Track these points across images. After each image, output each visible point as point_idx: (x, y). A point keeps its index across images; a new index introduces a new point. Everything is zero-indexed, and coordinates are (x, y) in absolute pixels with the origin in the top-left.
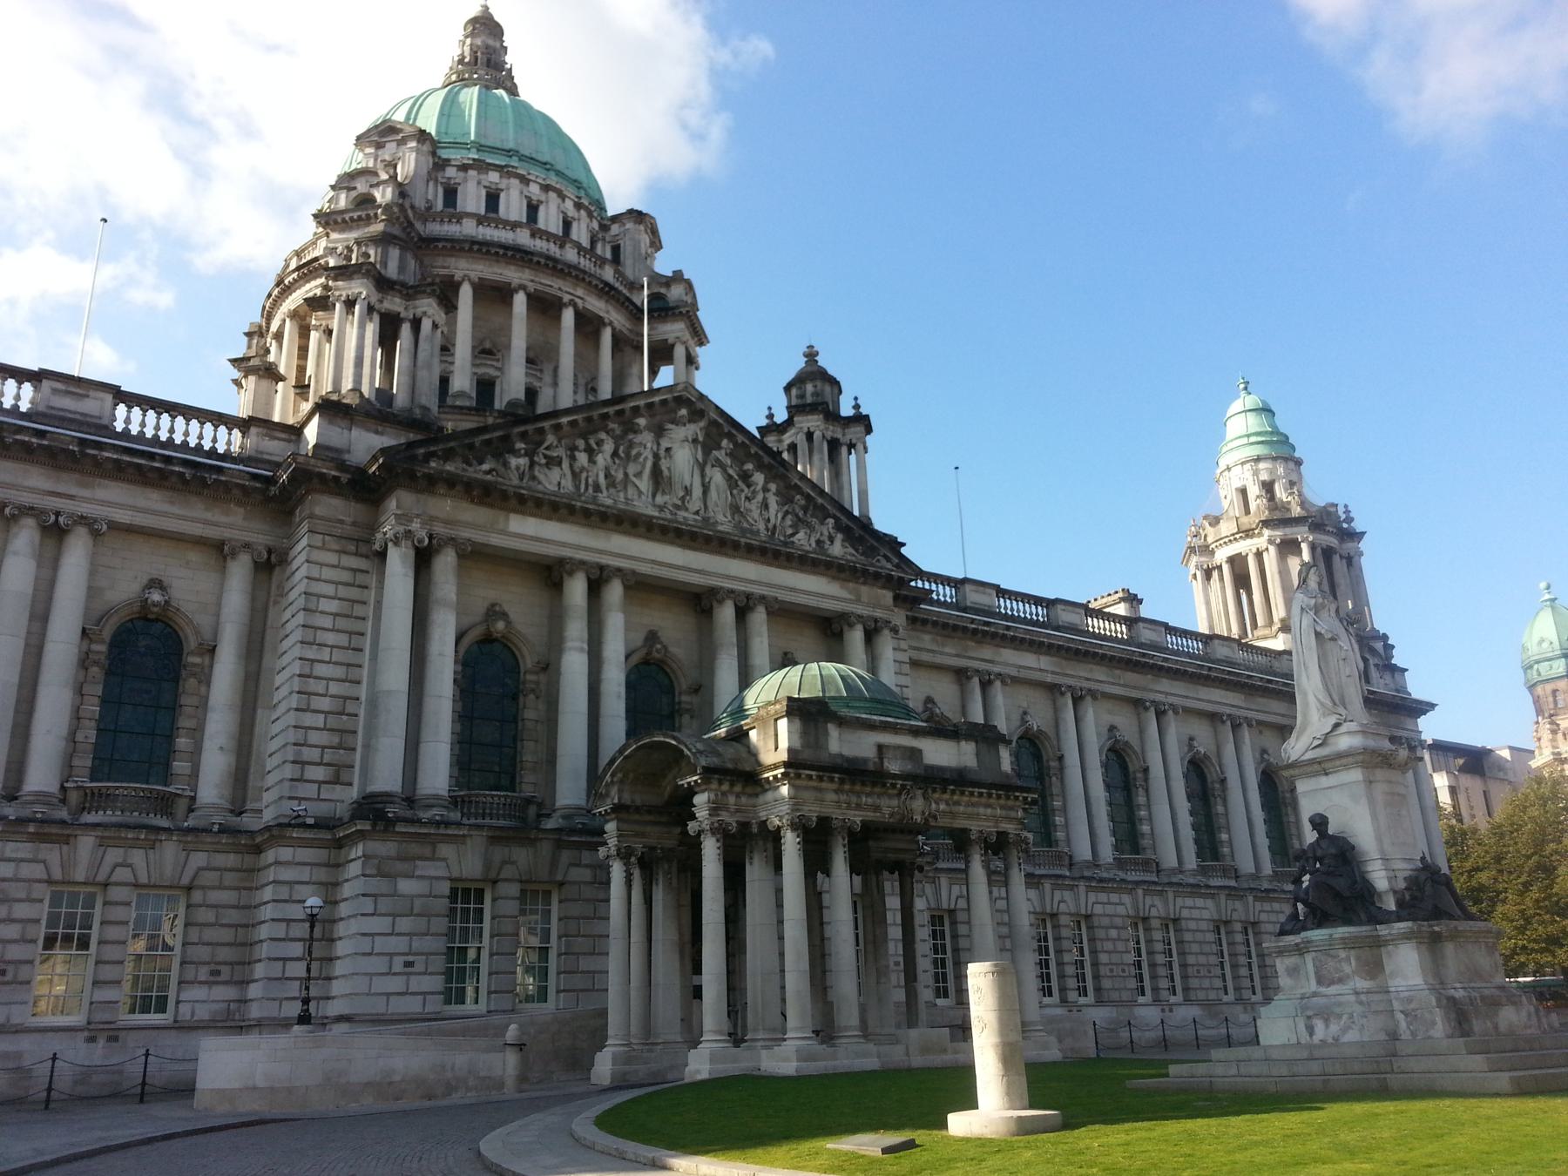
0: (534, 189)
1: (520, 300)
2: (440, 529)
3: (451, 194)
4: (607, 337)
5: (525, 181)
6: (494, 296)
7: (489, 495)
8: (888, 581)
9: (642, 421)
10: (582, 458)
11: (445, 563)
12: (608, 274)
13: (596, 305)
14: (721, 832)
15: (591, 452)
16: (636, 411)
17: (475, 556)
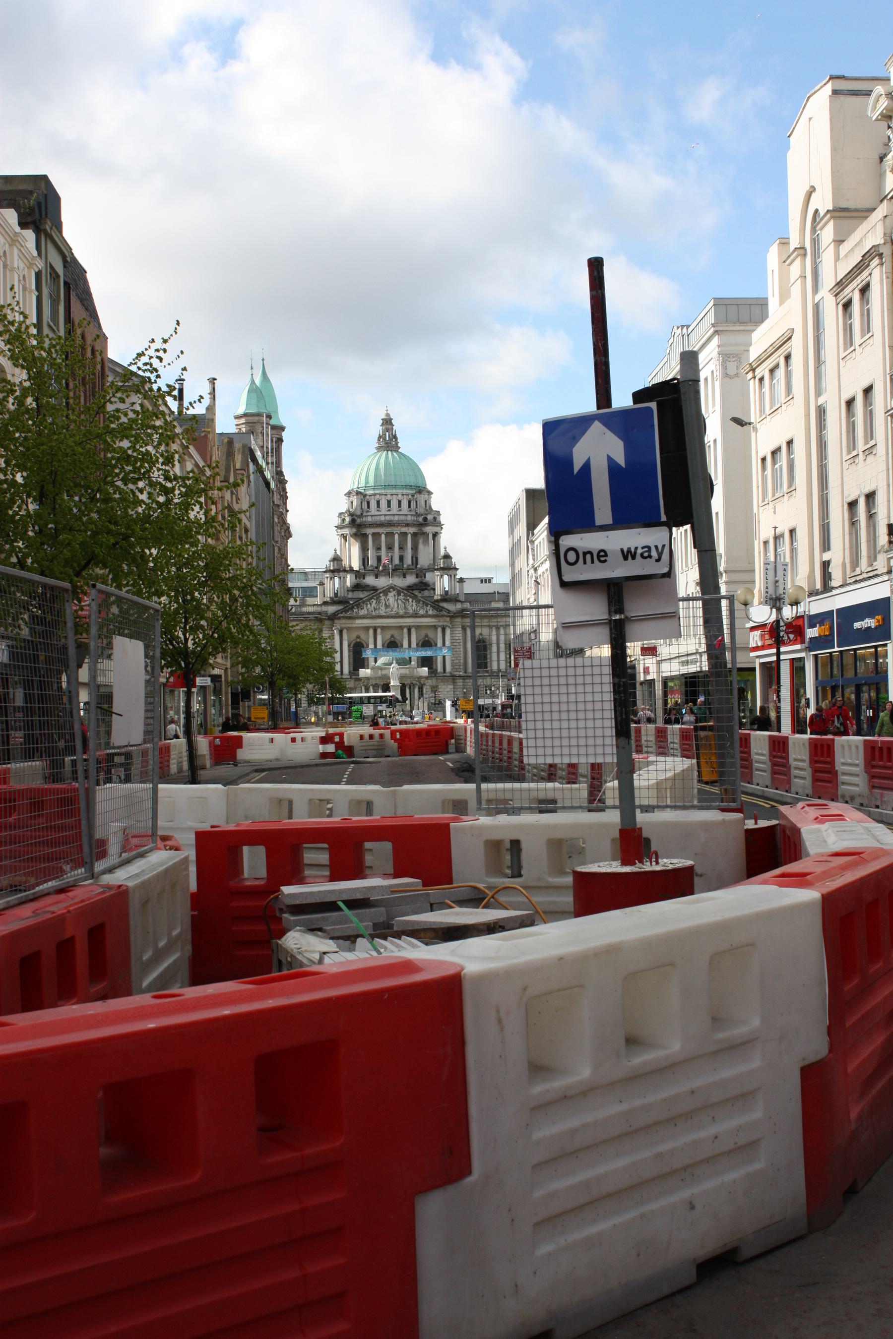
0: (389, 497)
1: (383, 536)
2: (343, 626)
3: (368, 503)
4: (409, 536)
5: (386, 495)
6: (376, 536)
7: (350, 618)
8: (447, 616)
9: (381, 595)
10: (369, 606)
11: (345, 632)
12: (409, 518)
13: (404, 530)
14: (364, 685)
15: (371, 604)
16: (381, 593)
17: (349, 629)
